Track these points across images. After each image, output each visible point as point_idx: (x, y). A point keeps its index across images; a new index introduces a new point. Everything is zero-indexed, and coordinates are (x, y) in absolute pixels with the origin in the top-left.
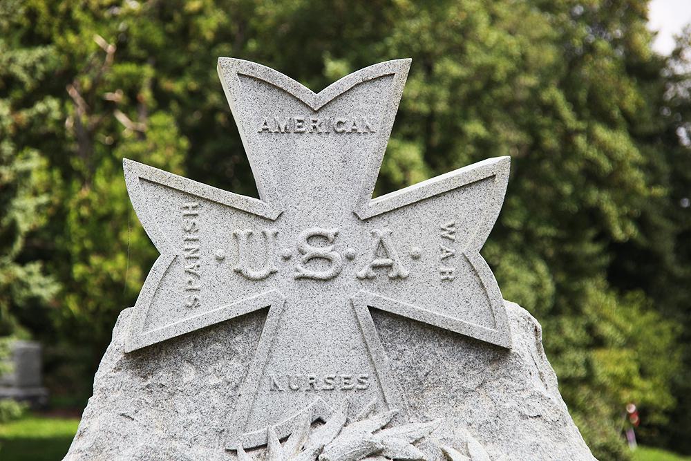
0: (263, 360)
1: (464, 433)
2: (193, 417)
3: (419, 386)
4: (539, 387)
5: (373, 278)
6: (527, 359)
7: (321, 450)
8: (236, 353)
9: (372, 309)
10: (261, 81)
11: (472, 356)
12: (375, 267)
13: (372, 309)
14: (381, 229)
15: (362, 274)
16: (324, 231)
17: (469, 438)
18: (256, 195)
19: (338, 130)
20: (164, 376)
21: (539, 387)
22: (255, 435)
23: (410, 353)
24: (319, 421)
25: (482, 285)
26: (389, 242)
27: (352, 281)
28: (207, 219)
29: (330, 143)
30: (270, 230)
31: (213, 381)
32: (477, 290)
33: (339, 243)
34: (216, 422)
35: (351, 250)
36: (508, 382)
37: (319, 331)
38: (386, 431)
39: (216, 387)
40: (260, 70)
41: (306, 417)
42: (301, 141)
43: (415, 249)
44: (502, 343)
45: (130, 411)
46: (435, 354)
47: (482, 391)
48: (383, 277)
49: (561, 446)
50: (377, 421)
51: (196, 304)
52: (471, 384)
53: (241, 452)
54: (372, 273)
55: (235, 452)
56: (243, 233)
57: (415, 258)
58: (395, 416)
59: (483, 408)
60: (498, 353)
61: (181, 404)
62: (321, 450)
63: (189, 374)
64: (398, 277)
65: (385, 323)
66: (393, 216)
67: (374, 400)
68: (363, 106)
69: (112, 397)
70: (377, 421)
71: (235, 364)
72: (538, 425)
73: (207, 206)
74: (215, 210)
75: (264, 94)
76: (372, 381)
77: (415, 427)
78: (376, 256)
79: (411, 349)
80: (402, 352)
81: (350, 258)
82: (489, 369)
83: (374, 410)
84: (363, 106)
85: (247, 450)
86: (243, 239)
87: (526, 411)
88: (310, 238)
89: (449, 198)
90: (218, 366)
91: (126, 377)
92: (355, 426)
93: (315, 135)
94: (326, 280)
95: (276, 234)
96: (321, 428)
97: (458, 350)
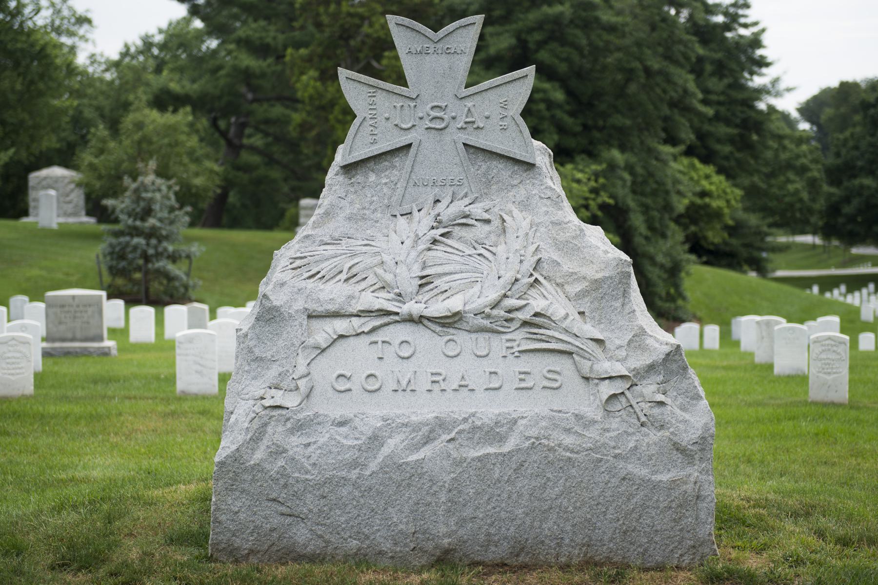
0: (409, 170)
1: (510, 206)
2: (375, 198)
3: (488, 184)
4: (550, 183)
5: (465, 128)
6: (544, 170)
7: (439, 215)
8: (396, 166)
9: (464, 144)
10: (408, 27)
11: (516, 168)
12: (466, 123)
13: (464, 144)
14: (469, 103)
15: (459, 126)
16: (440, 104)
17: (513, 208)
18: (406, 85)
19: (447, 52)
20: (359, 178)
21: (550, 183)
22: (406, 208)
23: (484, 167)
24: (438, 201)
25: (521, 131)
26: (473, 110)
27: (455, 130)
28: (380, 97)
29: (444, 60)
30: (412, 104)
31: (384, 181)
32: (519, 134)
33: (448, 110)
34: (386, 201)
35: (453, 114)
36: (534, 181)
37: (439, 157)
38: (472, 206)
39: (386, 184)
40: (407, 21)
41: (431, 200)
42: (427, 58)
43: (487, 114)
44: (531, 161)
45: (343, 195)
46: (497, 166)
47: (521, 185)
48: (470, 128)
49: (560, 212)
50: (467, 201)
51: (375, 142)
52: (515, 182)
53: (398, 216)
54: (465, 126)
55: (395, 216)
56: (399, 105)
57: (487, 118)
58: (477, 198)
59: (521, 193)
60: (530, 166)
61: (368, 192)
62: (439, 215)
63: (372, 177)
64: (478, 128)
65: (472, 151)
66: (476, 96)
67: (466, 190)
68: (459, 39)
69: (334, 188)
70: (467, 201)
71: (395, 172)
72: (548, 202)
73: (380, 91)
74: (384, 93)
75: (409, 33)
76: (465, 181)
77: (486, 204)
78: (467, 117)
79: (484, 165)
80: (480, 166)
81: (454, 118)
82: (525, 175)
83: (466, 196)
84: (459, 39)
85: (402, 215)
86: (399, 108)
87: (543, 195)
88: (433, 108)
89: (504, 87)
90: (387, 173)
91: (341, 178)
92: (456, 203)
93: (435, 55)
94: (441, 129)
95: (415, 106)
96: (439, 204)
97: (509, 164)
